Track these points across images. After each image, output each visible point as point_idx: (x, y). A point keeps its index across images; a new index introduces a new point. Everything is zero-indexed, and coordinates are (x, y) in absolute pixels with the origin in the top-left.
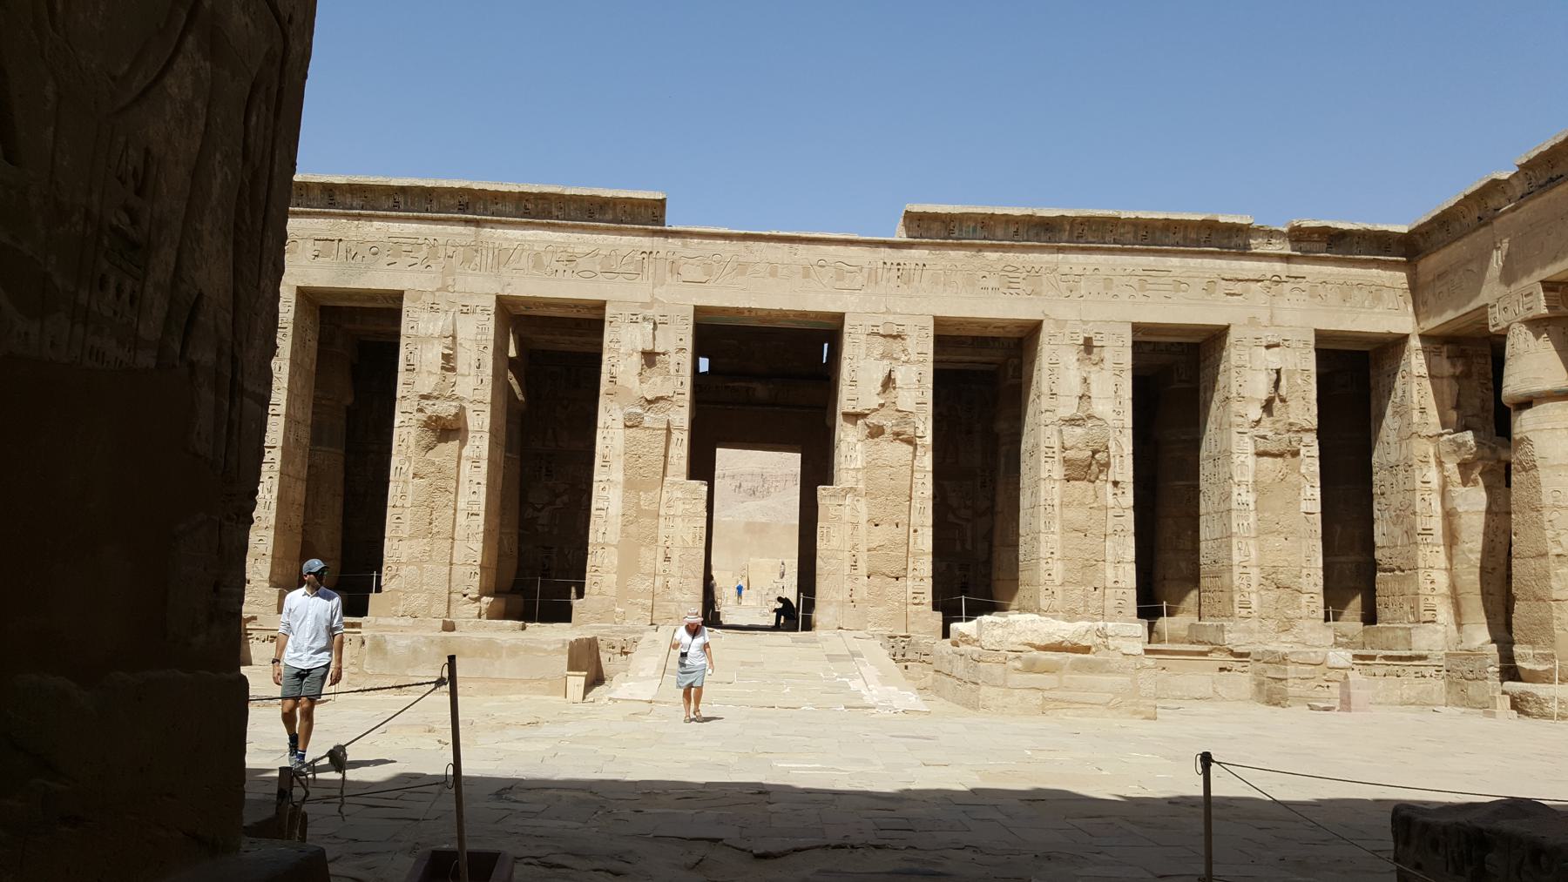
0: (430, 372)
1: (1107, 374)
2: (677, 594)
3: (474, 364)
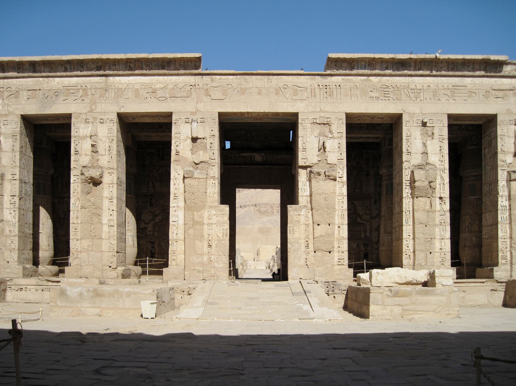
0: (86, 155)
1: (436, 141)
2: (216, 264)
3: (107, 149)
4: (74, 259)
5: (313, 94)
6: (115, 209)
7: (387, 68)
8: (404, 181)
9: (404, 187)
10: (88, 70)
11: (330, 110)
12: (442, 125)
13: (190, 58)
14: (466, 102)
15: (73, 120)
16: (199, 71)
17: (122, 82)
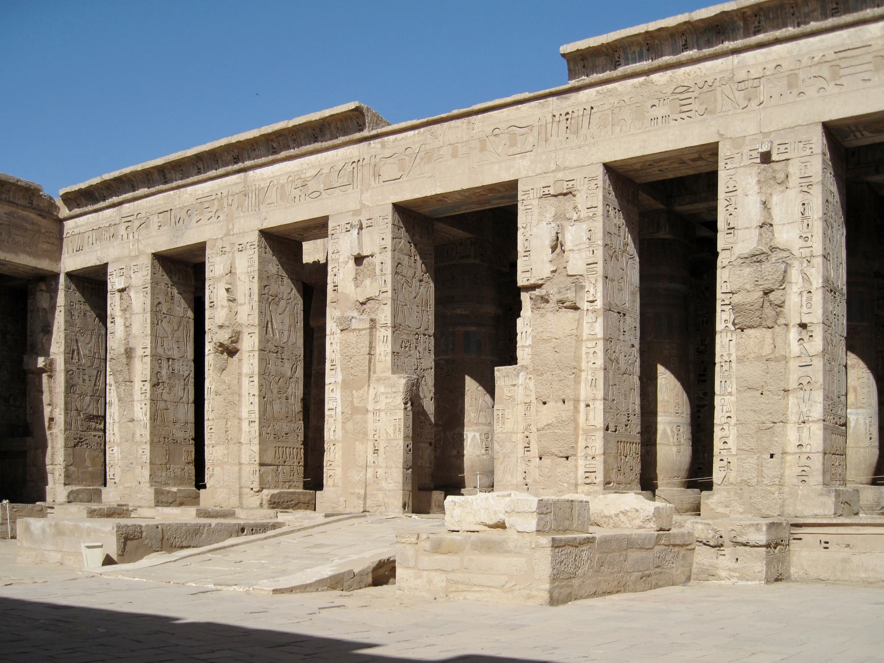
0: (223, 307)
2: (384, 484)
3: (247, 294)
4: (210, 477)
5: (543, 135)
6: (257, 394)
7: (686, 47)
8: (719, 296)
9: (719, 308)
10: (224, 166)
11: (575, 164)
12: (808, 152)
13: (342, 113)
14: (868, 84)
15: (208, 252)
16: (366, 133)
17: (265, 176)
